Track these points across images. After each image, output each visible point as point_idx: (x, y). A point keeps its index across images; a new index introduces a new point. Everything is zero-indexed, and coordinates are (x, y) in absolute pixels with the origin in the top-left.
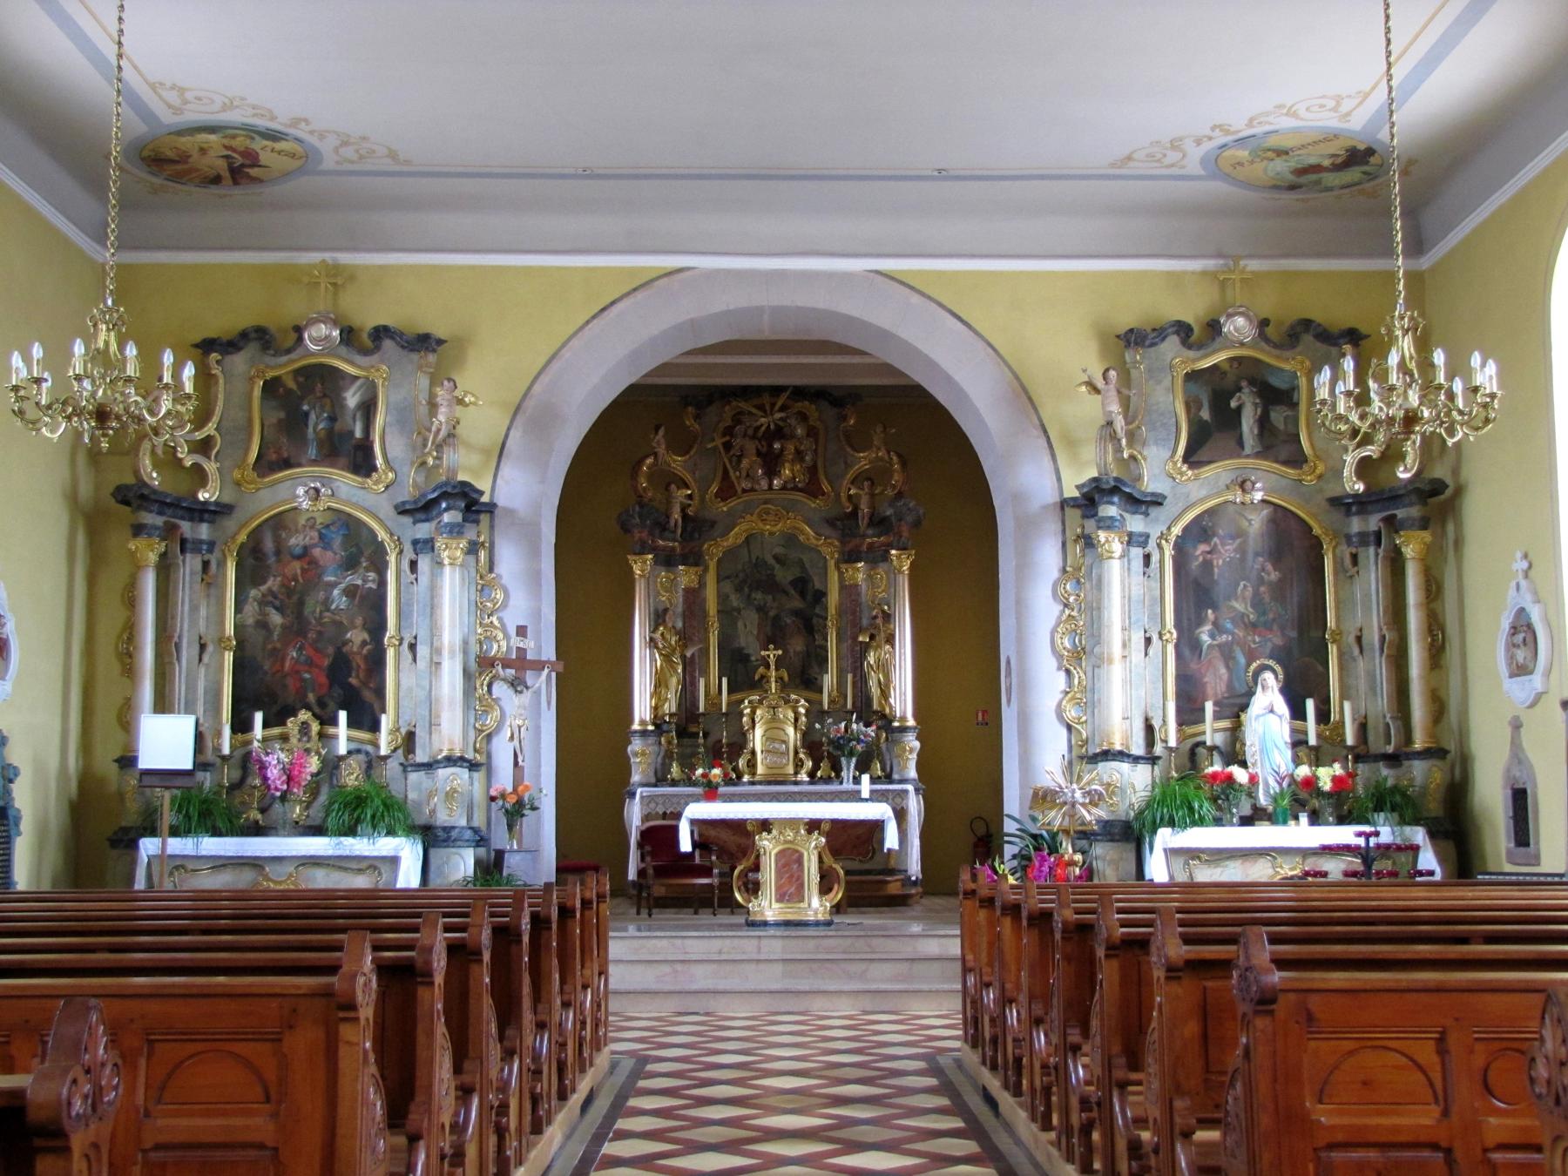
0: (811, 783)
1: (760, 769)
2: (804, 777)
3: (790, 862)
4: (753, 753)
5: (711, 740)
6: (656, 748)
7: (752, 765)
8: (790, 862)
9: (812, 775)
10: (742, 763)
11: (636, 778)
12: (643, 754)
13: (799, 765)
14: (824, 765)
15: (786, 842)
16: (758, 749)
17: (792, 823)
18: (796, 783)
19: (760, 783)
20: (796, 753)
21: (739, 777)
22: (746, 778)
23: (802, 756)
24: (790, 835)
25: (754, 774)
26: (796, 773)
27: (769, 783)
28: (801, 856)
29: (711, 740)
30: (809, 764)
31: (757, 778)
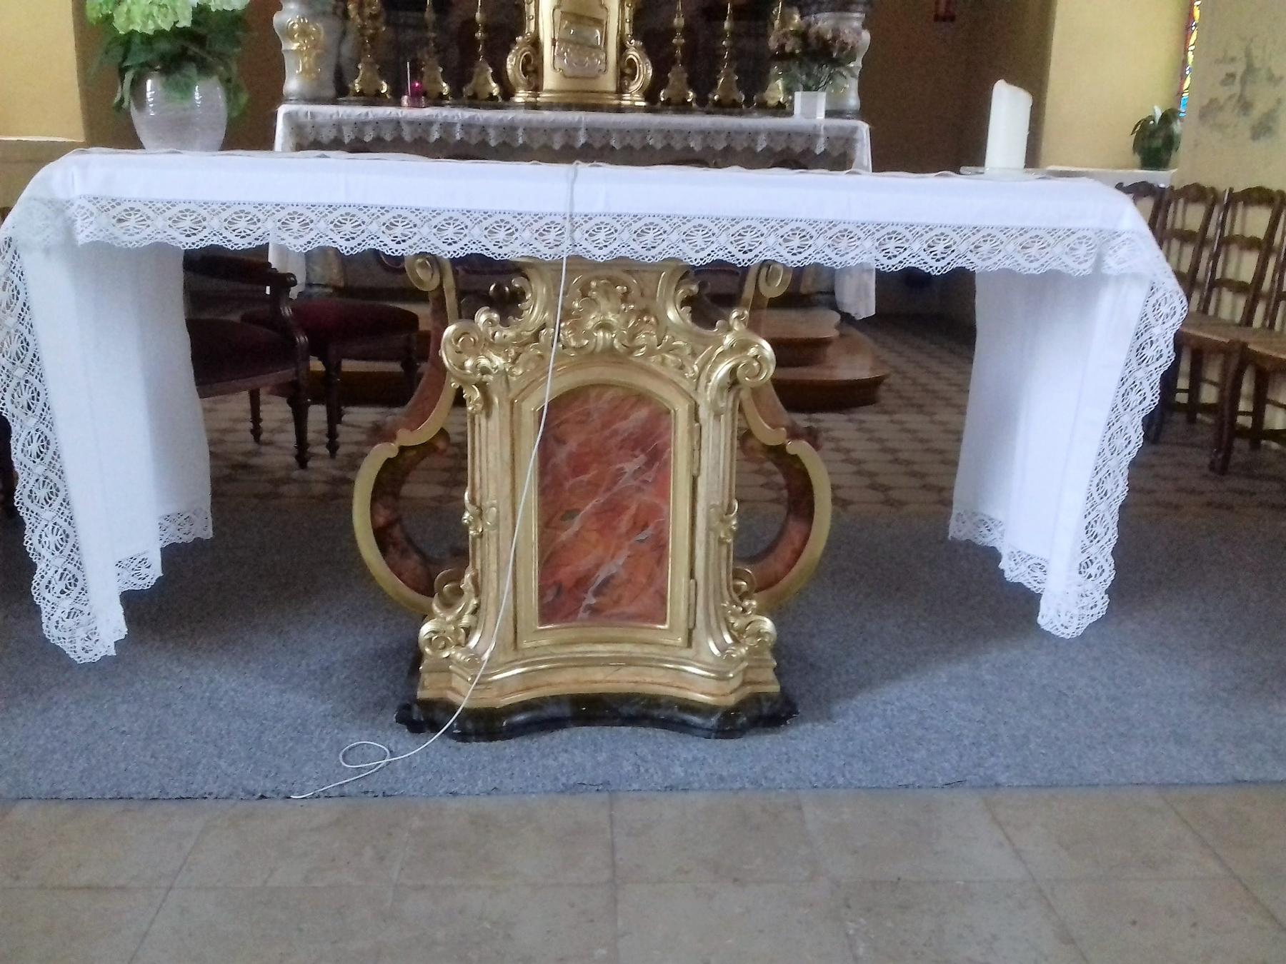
0: (647, 110)
1: (550, 79)
2: (633, 96)
3: (600, 451)
4: (536, 44)
5: (455, 19)
6: (336, 24)
7: (533, 69)
8: (600, 451)
9: (650, 94)
10: (512, 63)
11: (292, 84)
12: (304, 33)
13: (626, 72)
14: (677, 75)
15: (589, 356)
16: (546, 36)
17: (621, 278)
18: (619, 109)
19: (550, 106)
20: (622, 48)
21: (508, 93)
22: (521, 97)
23: (633, 54)
24: (605, 321)
25: (536, 88)
26: (621, 90)
27: (568, 107)
28: (662, 415)
29: (455, 19)
30: (646, 71)
31: (543, 97)
